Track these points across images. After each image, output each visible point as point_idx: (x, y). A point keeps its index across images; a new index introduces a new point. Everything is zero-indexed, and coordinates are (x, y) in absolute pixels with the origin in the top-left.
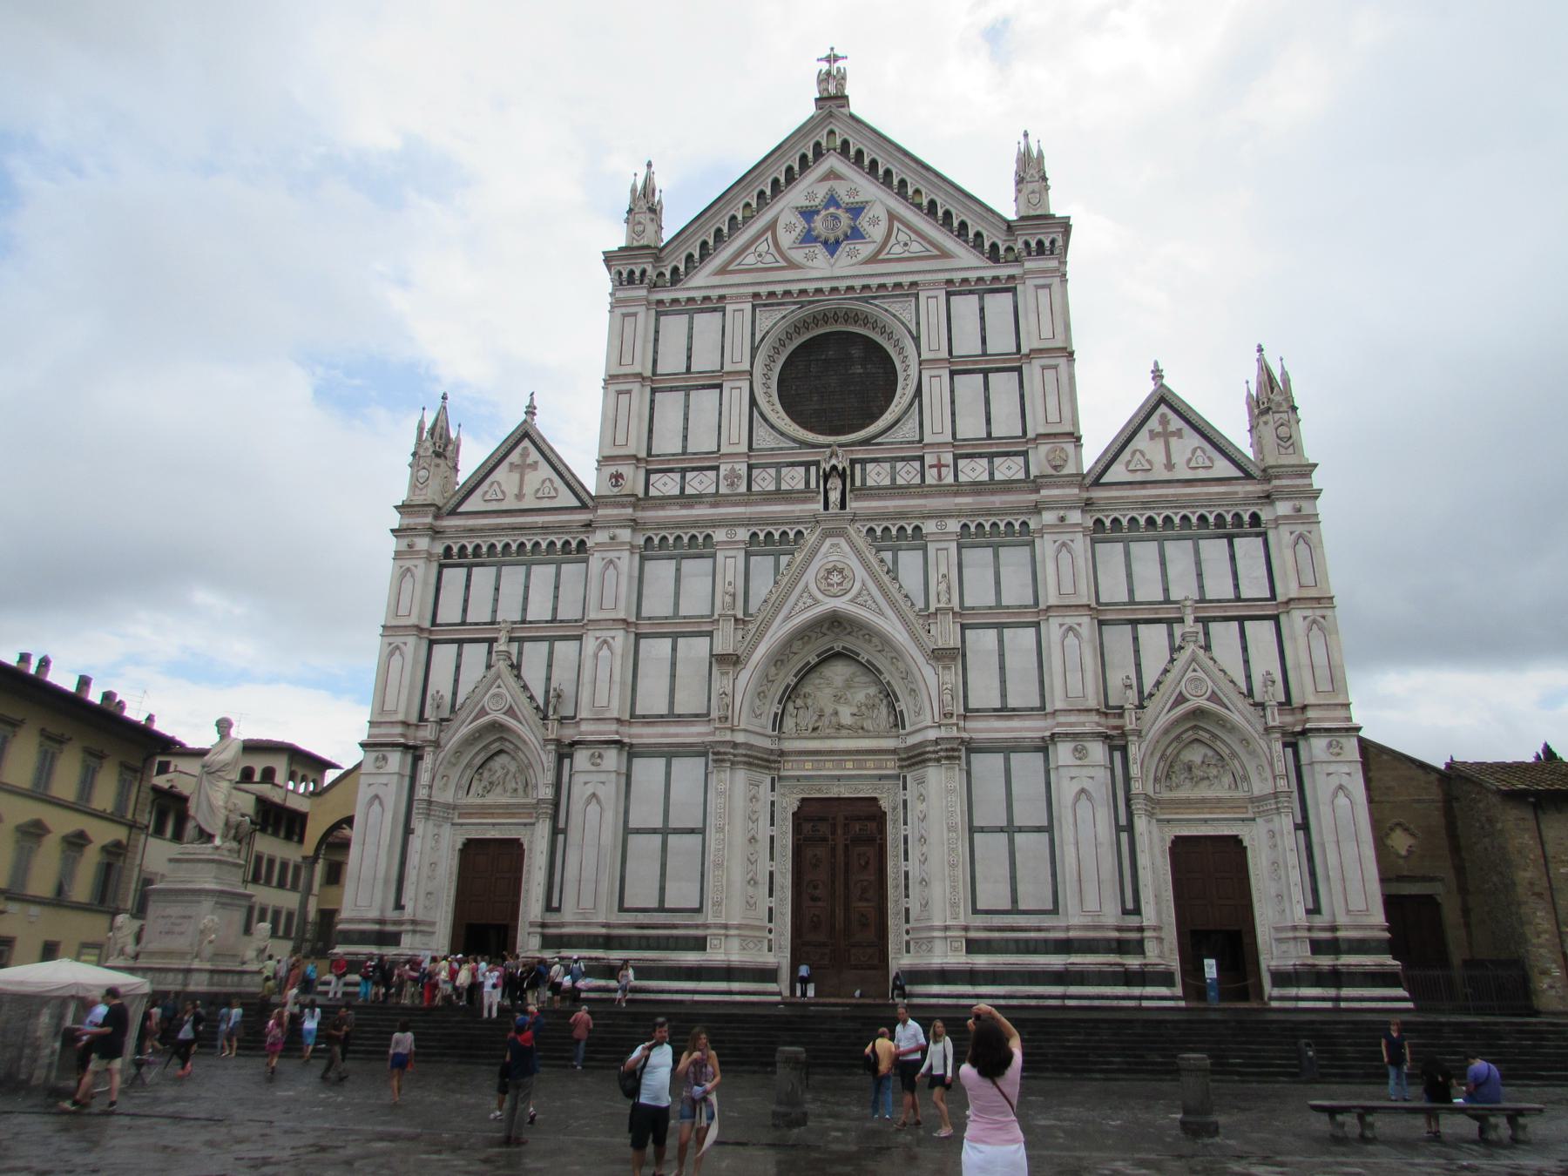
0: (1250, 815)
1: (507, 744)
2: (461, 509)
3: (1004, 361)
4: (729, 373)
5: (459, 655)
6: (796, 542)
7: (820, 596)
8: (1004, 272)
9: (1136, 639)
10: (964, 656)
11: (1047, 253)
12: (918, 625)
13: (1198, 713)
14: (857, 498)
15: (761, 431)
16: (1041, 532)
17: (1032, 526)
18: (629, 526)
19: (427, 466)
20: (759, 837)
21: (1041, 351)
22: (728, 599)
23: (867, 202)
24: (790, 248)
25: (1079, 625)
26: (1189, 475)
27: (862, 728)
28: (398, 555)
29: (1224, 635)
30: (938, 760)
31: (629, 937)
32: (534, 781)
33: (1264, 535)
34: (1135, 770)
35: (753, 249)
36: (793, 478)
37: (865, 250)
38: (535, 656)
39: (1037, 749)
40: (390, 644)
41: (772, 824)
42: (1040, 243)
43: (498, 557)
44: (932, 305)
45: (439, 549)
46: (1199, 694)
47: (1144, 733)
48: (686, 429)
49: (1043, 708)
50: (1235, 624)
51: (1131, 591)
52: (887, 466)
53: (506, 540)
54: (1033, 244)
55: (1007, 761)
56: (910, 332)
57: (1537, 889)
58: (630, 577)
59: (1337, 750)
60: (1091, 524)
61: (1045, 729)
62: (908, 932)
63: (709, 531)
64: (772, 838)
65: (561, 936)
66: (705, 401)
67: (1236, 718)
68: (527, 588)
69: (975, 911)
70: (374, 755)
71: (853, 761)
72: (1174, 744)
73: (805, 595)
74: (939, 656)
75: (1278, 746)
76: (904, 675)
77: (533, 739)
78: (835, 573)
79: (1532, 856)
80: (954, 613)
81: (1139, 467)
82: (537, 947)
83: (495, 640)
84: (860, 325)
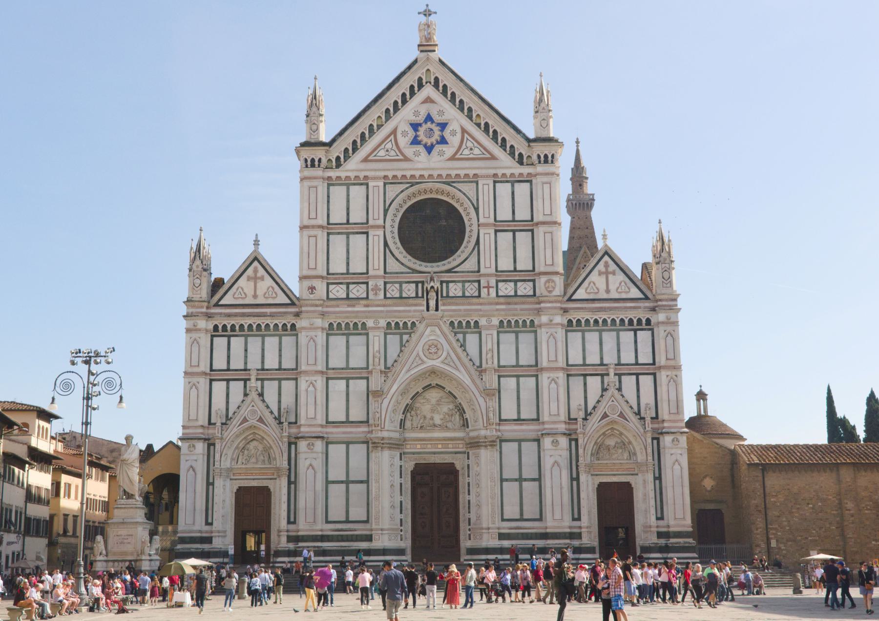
0: (636, 472)
1: (257, 436)
2: (221, 303)
3: (524, 226)
4: (373, 227)
5: (228, 388)
6: (412, 328)
7: (425, 359)
8: (525, 170)
9: (585, 384)
10: (499, 392)
11: (550, 162)
12: (475, 374)
13: (613, 422)
14: (444, 305)
15: (390, 260)
16: (540, 326)
17: (536, 322)
18: (320, 318)
19: (198, 277)
20: (395, 484)
21: (544, 223)
22: (377, 360)
23: (449, 120)
24: (404, 148)
25: (558, 378)
26: (617, 296)
27: (446, 427)
28: (188, 331)
29: (629, 382)
30: (486, 446)
31: (332, 536)
32: (274, 456)
33: (652, 330)
34: (581, 451)
35: (383, 146)
36: (409, 290)
37: (449, 151)
38: (271, 389)
39: (534, 440)
40: (189, 383)
41: (401, 477)
42: (546, 156)
43: (245, 332)
44: (486, 187)
45: (211, 327)
46: (614, 413)
47: (586, 433)
48: (348, 258)
49: (538, 419)
50: (634, 377)
51: (584, 358)
52: (460, 285)
53: (249, 322)
54: (542, 157)
55: (520, 446)
56: (473, 205)
57: (759, 509)
58: (322, 346)
59: (677, 443)
60: (566, 322)
61: (539, 430)
62: (470, 530)
63: (364, 321)
64: (401, 484)
65: (298, 536)
66: (358, 241)
67: (631, 425)
68: (263, 350)
69: (503, 520)
70: (188, 444)
71: (442, 444)
72: (602, 437)
73: (417, 358)
74: (488, 393)
75: (649, 440)
76: (469, 401)
77: (274, 435)
78: (433, 346)
79: (758, 494)
80: (495, 370)
81: (592, 291)
82: (286, 542)
83: (249, 379)
84: (445, 196)
